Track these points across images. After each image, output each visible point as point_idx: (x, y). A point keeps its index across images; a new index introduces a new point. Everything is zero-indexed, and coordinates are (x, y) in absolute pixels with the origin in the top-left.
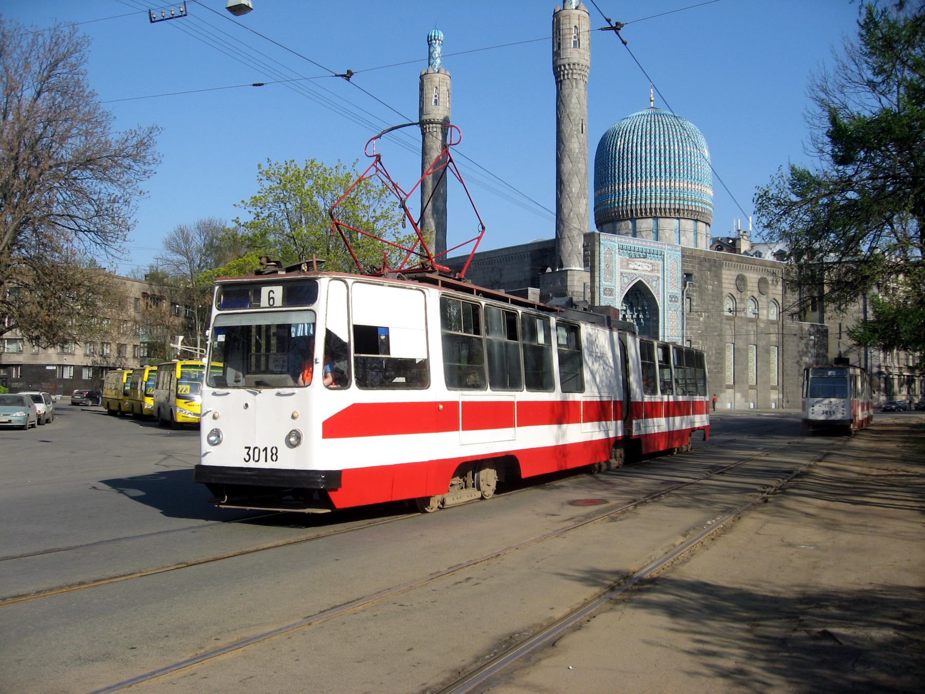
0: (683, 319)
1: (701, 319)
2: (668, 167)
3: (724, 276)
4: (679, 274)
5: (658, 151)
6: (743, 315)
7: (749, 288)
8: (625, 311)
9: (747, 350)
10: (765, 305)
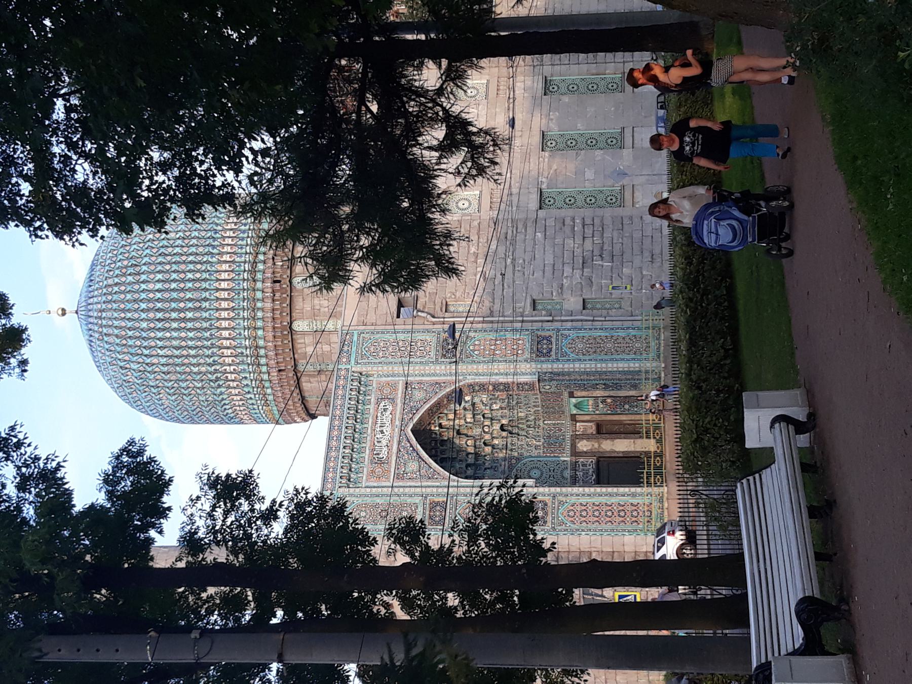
2: (190, 305)
5: (160, 325)
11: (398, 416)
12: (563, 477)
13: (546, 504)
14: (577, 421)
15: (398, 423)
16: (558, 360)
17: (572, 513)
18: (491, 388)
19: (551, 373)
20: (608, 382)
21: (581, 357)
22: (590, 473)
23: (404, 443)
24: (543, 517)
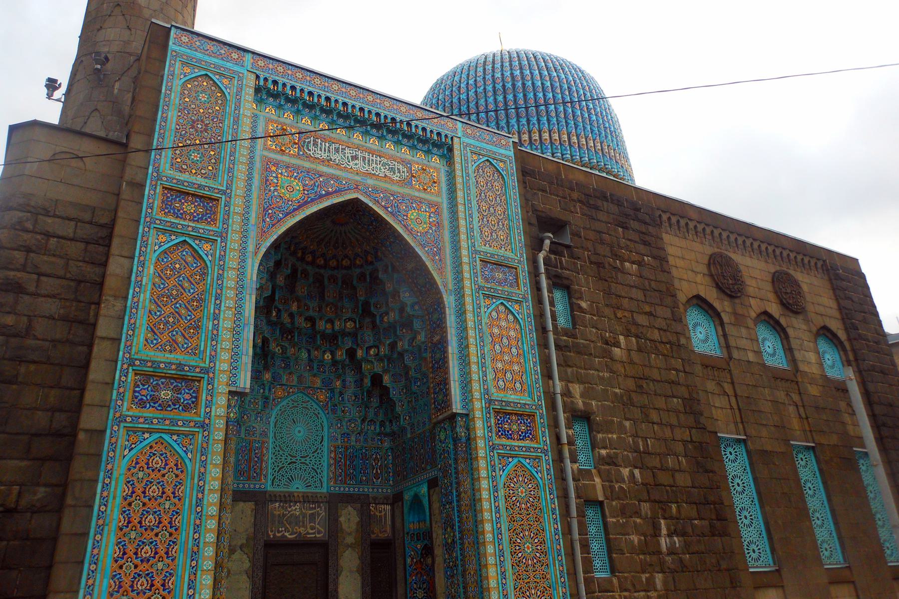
0: (543, 345)
1: (616, 351)
3: (670, 250)
4: (515, 209)
6: (751, 357)
7: (751, 290)
8: (354, 335)
9: (788, 456)
10: (806, 336)
11: (383, 185)
12: (291, 479)
13: (186, 408)
14: (392, 505)
15: (370, 182)
16: (493, 448)
17: (157, 462)
18: (436, 338)
19: (469, 439)
21: (501, 493)
23: (332, 186)
24: (154, 400)
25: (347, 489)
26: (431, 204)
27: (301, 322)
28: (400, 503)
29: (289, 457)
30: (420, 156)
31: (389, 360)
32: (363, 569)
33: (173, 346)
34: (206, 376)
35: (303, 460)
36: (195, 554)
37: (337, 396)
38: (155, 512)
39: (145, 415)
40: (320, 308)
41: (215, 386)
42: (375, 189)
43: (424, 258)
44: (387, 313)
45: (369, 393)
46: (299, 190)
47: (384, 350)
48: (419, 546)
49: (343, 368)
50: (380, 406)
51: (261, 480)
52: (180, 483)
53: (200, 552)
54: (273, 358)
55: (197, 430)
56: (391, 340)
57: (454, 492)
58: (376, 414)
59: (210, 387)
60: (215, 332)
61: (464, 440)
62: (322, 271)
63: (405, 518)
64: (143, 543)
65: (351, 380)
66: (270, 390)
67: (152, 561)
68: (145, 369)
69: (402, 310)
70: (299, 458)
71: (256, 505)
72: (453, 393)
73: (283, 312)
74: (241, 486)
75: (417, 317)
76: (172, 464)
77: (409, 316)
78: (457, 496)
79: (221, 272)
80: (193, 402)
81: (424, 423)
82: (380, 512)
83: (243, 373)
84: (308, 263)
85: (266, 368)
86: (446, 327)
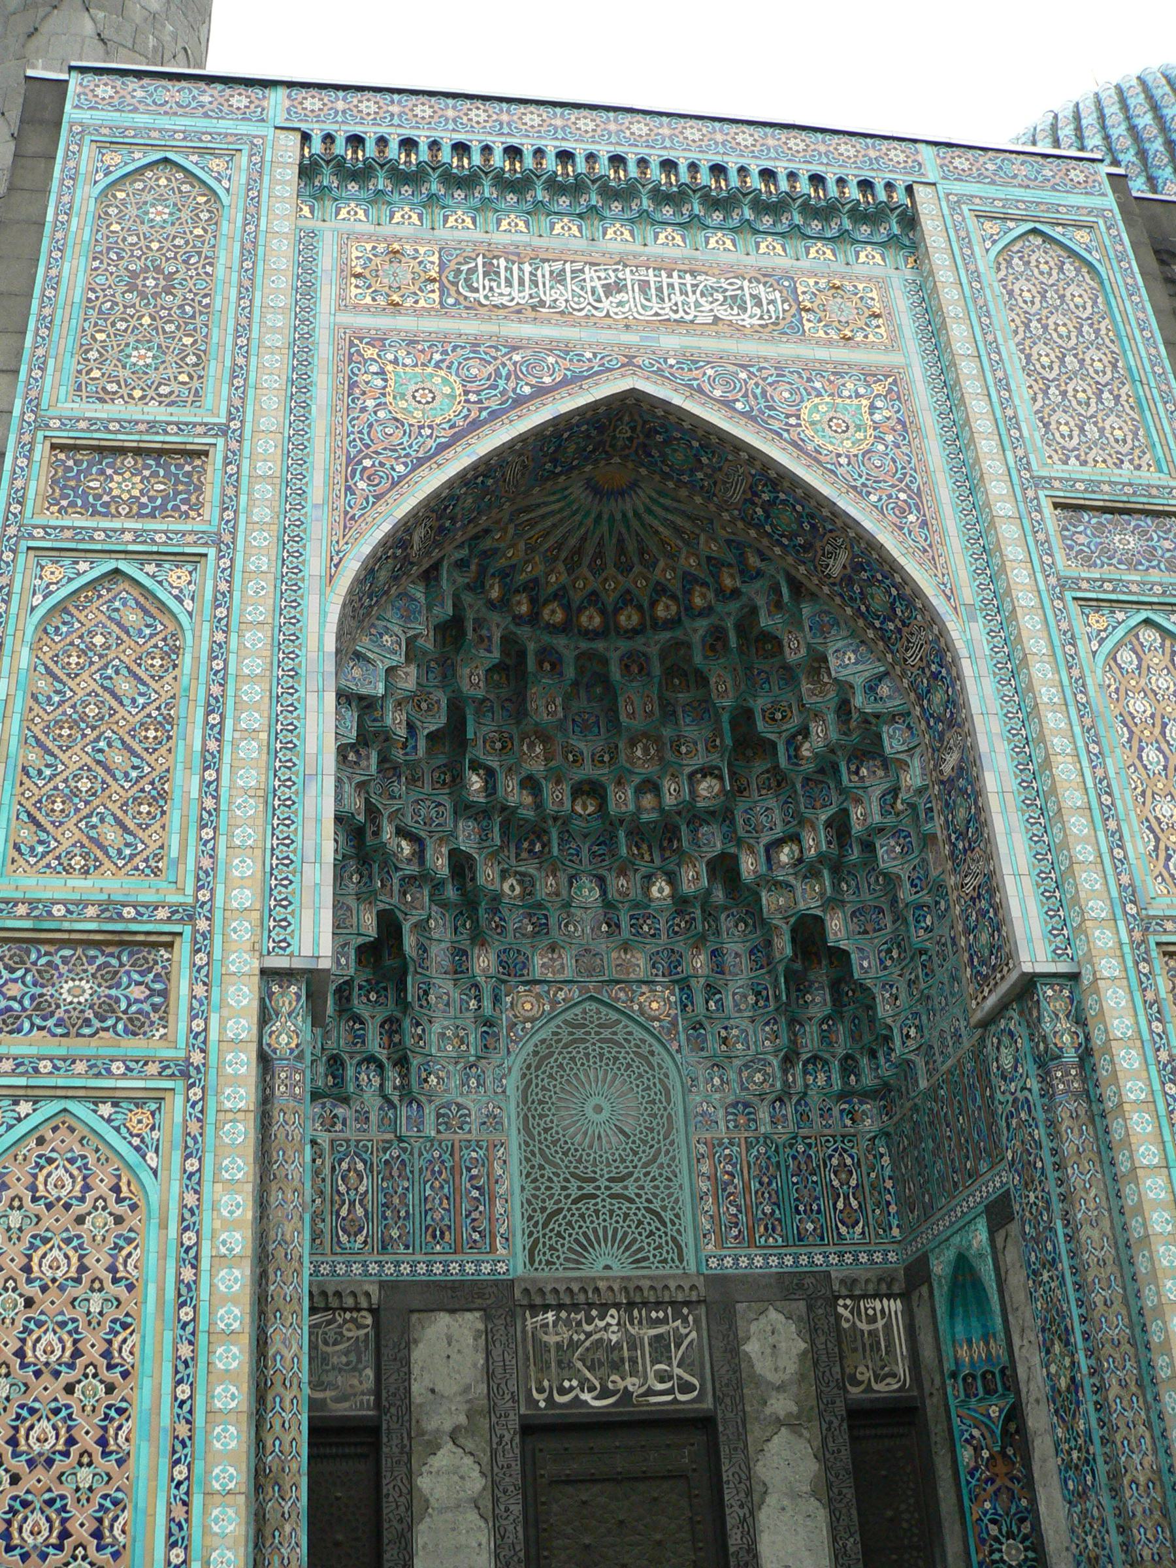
11: (710, 344)
12: (585, 1246)
13: (135, 1027)
14: (905, 1296)
15: (670, 342)
20: (1088, 1401)
22: (617, 1382)
24: (44, 1009)
25: (759, 1261)
26: (869, 375)
27: (557, 797)
28: (924, 1290)
29: (575, 1183)
30: (820, 255)
31: (838, 870)
32: (830, 1486)
33: (94, 852)
34: (188, 930)
35: (617, 1188)
36: (181, 1448)
37: (699, 999)
38: (62, 1325)
39: (15, 1051)
40: (614, 751)
41: (217, 955)
42: (691, 361)
43: (868, 524)
44: (805, 732)
45: (797, 982)
46: (452, 396)
47: (814, 842)
48: (994, 1412)
49: (710, 914)
50: (837, 1013)
51: (493, 1249)
52: (129, 1241)
53: (199, 1437)
54: (496, 911)
55: (169, 1084)
56: (831, 811)
57: (1059, 1225)
58: (826, 1038)
59: (201, 959)
60: (209, 803)
61: (1070, 1056)
62: (600, 645)
63: (943, 1326)
64: (32, 1411)
65: (738, 948)
66: (496, 999)
67: (60, 1464)
68: (10, 924)
69: (844, 708)
70: (603, 1183)
71: (487, 1318)
72: (1015, 910)
73: (500, 777)
74: (438, 1269)
75: (893, 718)
76: (103, 1189)
77: (866, 720)
78: (1069, 1238)
79: (220, 637)
80: (155, 1008)
81: (957, 1036)
82: (872, 1320)
83: (307, 916)
84: (552, 629)
85: (478, 938)
86: (970, 718)
